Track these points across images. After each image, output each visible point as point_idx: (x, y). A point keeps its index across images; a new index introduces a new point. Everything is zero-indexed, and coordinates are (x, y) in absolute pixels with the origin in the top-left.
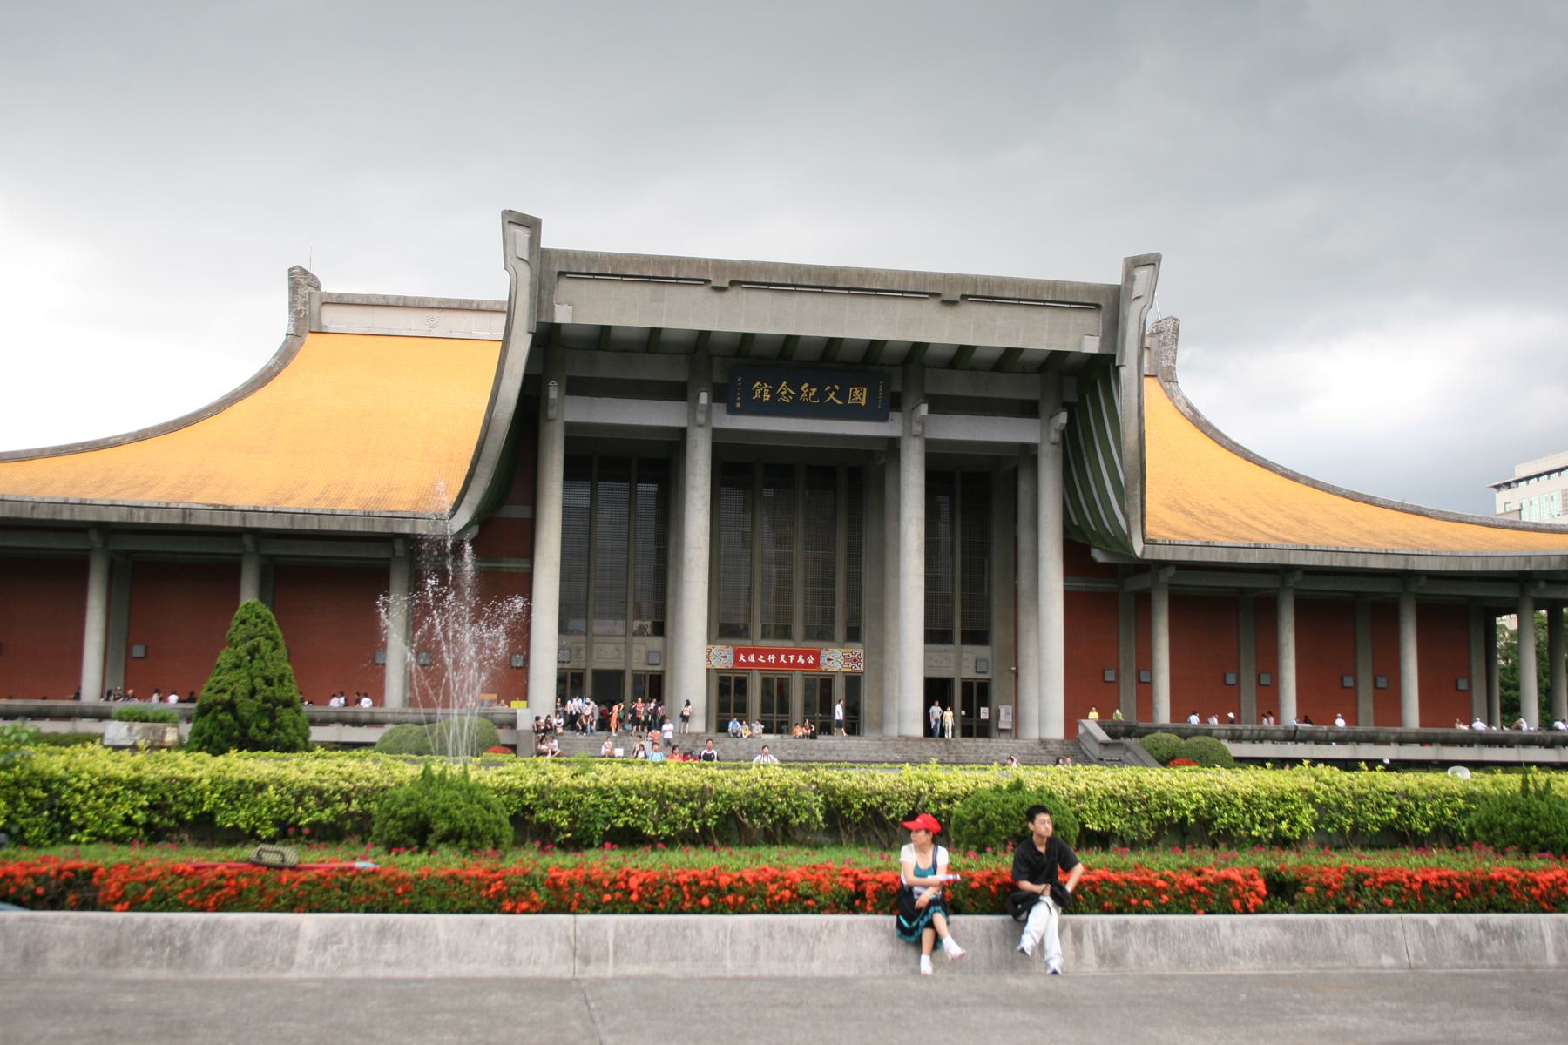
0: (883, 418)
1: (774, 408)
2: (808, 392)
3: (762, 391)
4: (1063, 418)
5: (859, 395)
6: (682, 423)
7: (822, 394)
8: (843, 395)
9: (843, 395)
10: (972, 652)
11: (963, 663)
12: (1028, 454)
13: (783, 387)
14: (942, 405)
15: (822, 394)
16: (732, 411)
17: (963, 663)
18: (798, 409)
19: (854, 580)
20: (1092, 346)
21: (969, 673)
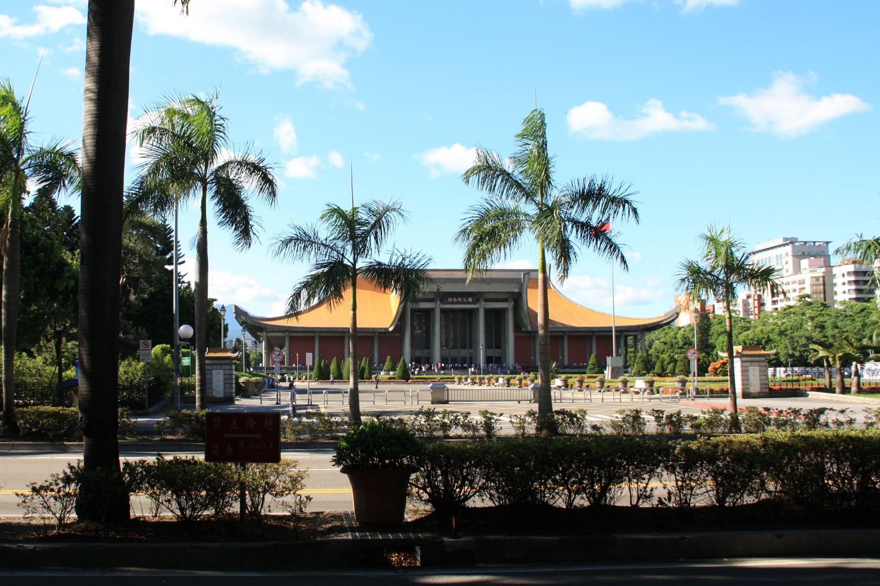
0: (475, 304)
1: (453, 303)
2: (459, 299)
3: (450, 300)
4: (513, 303)
5: (470, 300)
6: (434, 307)
7: (462, 300)
8: (467, 300)
9: (467, 300)
10: (497, 351)
11: (494, 353)
12: (507, 309)
13: (455, 299)
14: (487, 300)
15: (462, 300)
16: (444, 304)
17: (494, 353)
18: (458, 303)
19: (471, 335)
20: (516, 290)
21: (497, 355)
